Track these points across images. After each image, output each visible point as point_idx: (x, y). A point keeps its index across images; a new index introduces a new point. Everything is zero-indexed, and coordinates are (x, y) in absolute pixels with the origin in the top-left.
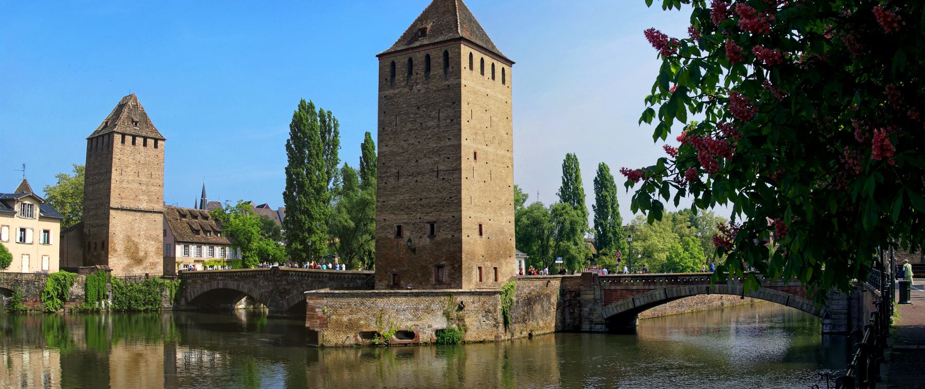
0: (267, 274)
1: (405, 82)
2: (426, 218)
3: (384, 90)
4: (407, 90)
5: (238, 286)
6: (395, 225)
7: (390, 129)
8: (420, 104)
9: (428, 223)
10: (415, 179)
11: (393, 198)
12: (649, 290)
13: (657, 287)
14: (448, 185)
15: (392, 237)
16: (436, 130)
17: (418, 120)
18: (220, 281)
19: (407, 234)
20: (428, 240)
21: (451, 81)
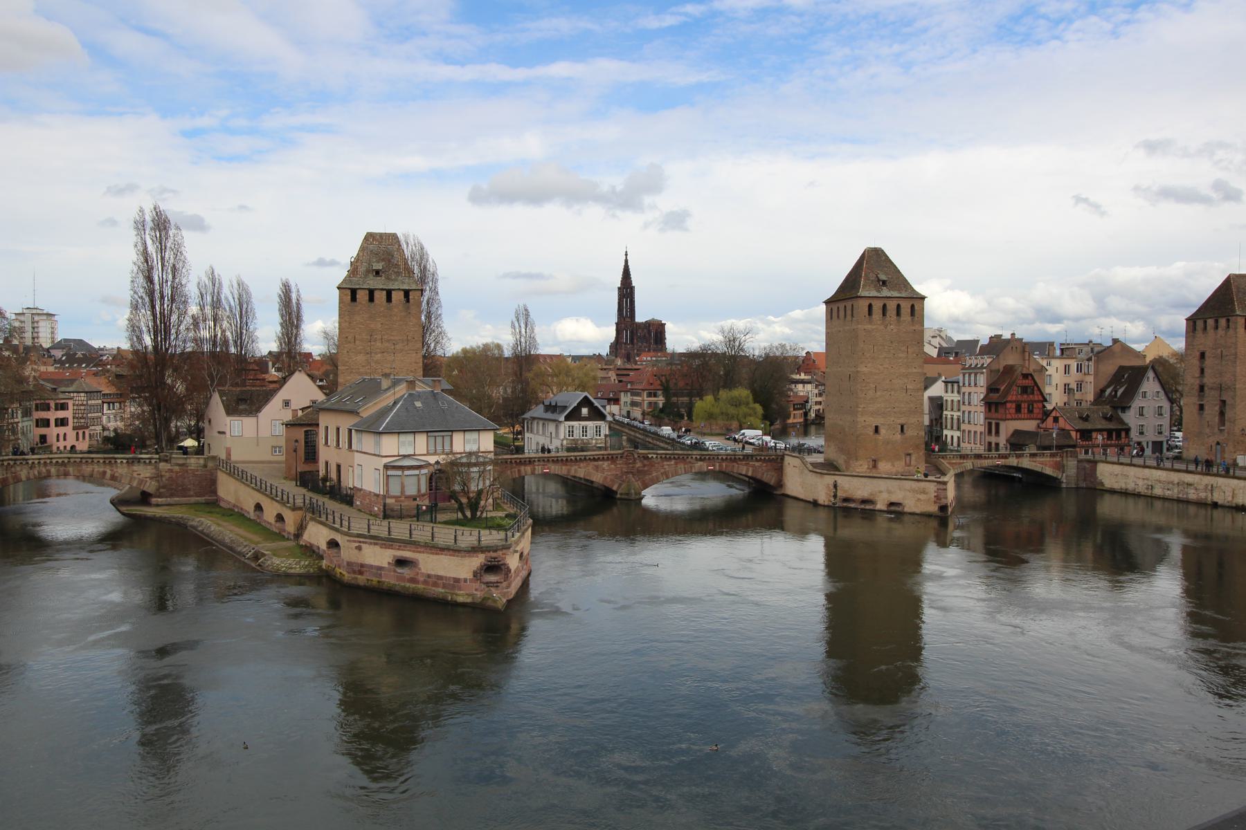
0: (617, 457)
4: (882, 327)
5: (569, 471)
6: (874, 425)
11: (871, 406)
12: (963, 463)
13: (968, 461)
15: (872, 433)
16: (905, 360)
17: (892, 352)
18: (536, 467)
19: (882, 431)
20: (899, 436)
21: (917, 327)
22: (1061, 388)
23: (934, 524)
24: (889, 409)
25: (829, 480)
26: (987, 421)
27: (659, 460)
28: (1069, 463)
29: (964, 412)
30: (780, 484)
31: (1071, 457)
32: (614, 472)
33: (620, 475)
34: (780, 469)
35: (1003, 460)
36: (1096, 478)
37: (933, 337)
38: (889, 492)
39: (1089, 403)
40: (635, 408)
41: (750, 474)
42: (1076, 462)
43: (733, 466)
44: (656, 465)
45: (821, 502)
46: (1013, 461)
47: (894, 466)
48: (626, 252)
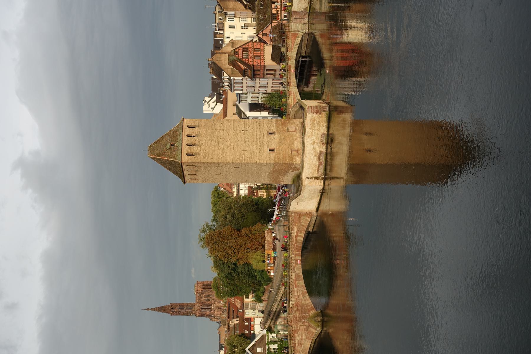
1: (199, 147)
2: (266, 136)
3: (200, 159)
6: (269, 152)
7: (221, 155)
8: (211, 139)
9: (268, 135)
10: (247, 142)
11: (255, 154)
12: (293, 93)
13: (292, 90)
14: (251, 125)
16: (225, 131)
17: (219, 140)
19: (273, 146)
22: (244, 30)
23: (334, 114)
24: (258, 141)
25: (305, 182)
26: (265, 77)
27: (294, 299)
28: (292, 28)
29: (259, 90)
30: (309, 214)
31: (289, 27)
32: (303, 332)
33: (304, 326)
34: (300, 215)
35: (291, 68)
36: (302, 12)
37: (209, 106)
38: (313, 143)
39: (254, 14)
40: (257, 307)
41: (303, 235)
42: (292, 24)
43: (297, 246)
44: (298, 301)
45: (321, 187)
46: (292, 63)
47: (296, 139)
48: (146, 309)
